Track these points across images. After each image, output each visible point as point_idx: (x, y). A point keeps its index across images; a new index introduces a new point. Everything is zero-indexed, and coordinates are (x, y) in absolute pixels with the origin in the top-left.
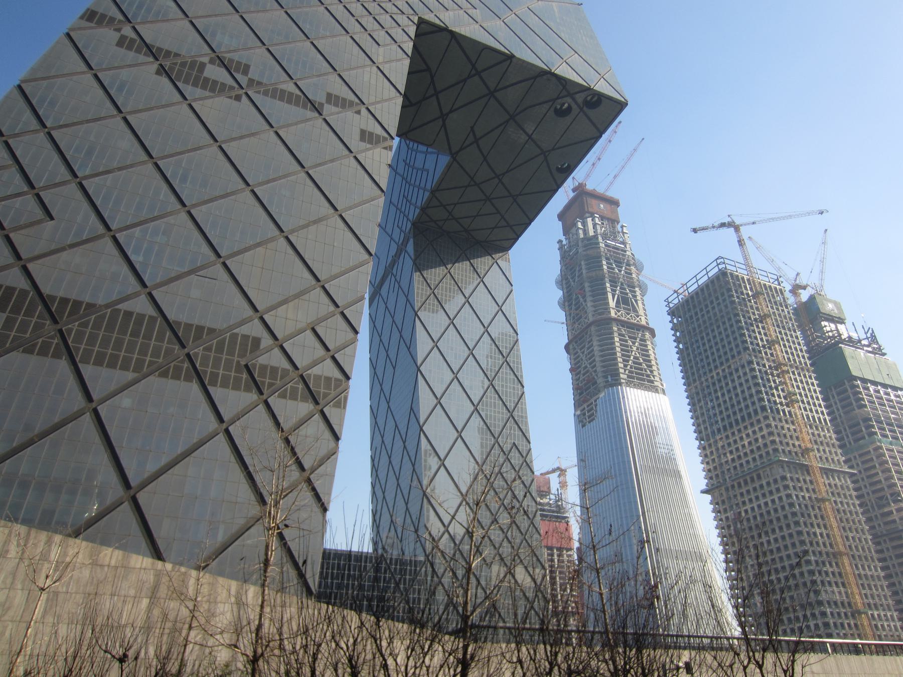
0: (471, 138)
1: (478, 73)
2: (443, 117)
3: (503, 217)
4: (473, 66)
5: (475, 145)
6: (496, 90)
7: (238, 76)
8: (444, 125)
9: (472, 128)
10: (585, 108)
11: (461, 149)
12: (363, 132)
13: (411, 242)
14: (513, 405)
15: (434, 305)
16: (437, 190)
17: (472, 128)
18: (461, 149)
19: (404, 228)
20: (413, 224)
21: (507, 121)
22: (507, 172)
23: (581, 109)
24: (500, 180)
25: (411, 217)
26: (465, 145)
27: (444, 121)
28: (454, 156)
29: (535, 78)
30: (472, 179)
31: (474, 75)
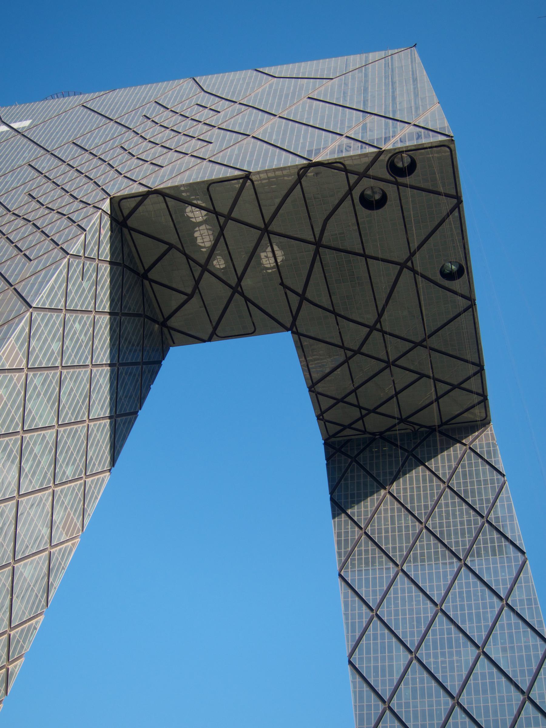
3: (435, 380)
5: (305, 302)
6: (267, 225)
8: (247, 299)
9: (282, 284)
10: (400, 180)
14: (528, 679)
17: (282, 284)
18: (295, 318)
21: (317, 252)
22: (380, 315)
27: (242, 294)
28: (292, 328)
29: (299, 181)
31: (226, 223)
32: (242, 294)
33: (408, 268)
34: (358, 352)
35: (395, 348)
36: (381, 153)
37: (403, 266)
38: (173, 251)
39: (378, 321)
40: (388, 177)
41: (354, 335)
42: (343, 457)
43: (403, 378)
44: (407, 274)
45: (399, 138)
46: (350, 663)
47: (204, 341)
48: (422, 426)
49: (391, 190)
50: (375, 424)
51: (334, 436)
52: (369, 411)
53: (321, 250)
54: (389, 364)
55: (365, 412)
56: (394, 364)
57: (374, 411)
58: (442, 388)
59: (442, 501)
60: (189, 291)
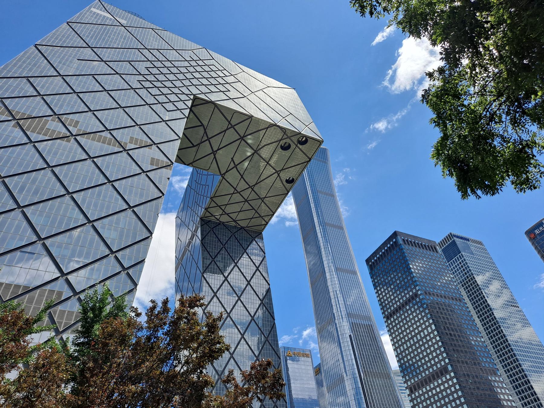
0: (232, 165)
1: (233, 127)
2: (214, 153)
3: (256, 212)
4: (229, 122)
6: (244, 136)
7: (70, 128)
8: (215, 157)
9: (232, 159)
10: (299, 145)
11: (227, 172)
12: (153, 159)
13: (200, 228)
15: (214, 268)
16: (214, 197)
18: (227, 172)
19: (195, 222)
20: (201, 219)
22: (256, 184)
23: (297, 145)
24: (253, 189)
25: (199, 214)
26: (229, 169)
27: (215, 155)
30: (235, 189)
32: (215, 155)
34: (239, 193)
37: (277, 172)
38: (202, 128)
41: (242, 185)
42: (208, 227)
43: (246, 206)
44: (276, 175)
47: (185, 164)
48: (239, 225)
49: (293, 146)
50: (224, 219)
54: (246, 201)
55: (224, 213)
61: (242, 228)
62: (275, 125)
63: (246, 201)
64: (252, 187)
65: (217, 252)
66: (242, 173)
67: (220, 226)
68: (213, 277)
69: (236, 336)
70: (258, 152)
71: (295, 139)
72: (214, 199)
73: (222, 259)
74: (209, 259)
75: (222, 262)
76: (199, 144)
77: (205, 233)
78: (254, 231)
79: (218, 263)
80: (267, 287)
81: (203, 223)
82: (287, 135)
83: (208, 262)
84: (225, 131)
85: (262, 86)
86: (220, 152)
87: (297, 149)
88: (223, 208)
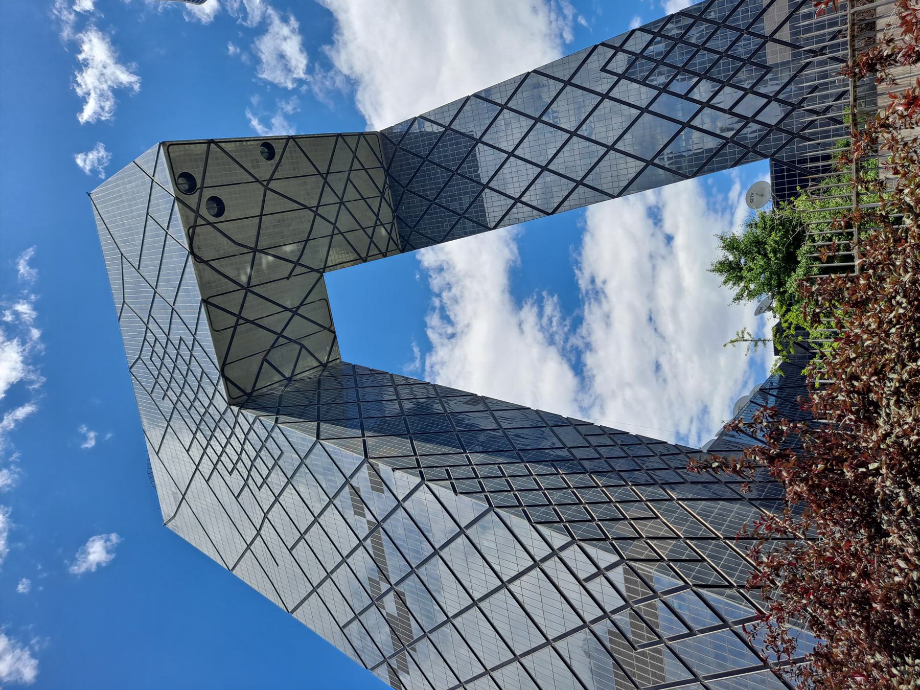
2: (295, 312)
3: (350, 170)
8: (302, 304)
10: (199, 186)
18: (313, 270)
21: (262, 251)
22: (306, 207)
23: (202, 188)
27: (298, 308)
28: (321, 272)
32: (298, 308)
33: (268, 184)
34: (334, 224)
35: (329, 197)
36: (177, 199)
37: (267, 188)
39: (310, 209)
40: (197, 194)
41: (323, 228)
42: (412, 237)
43: (351, 194)
44: (273, 185)
45: (164, 175)
46: (553, 212)
49: (208, 194)
50: (386, 214)
51: (397, 245)
52: (378, 219)
53: (259, 248)
54: (342, 203)
55: (378, 222)
56: (341, 199)
57: (377, 215)
58: (356, 165)
59: (437, 161)
60: (298, 347)
61: (387, 173)
62: (192, 252)
63: (342, 203)
64: (315, 211)
65: (446, 213)
66: (301, 245)
67: (401, 217)
68: (491, 210)
69: (576, 146)
70: (253, 246)
71: (192, 200)
72: (364, 255)
73: (455, 200)
74: (464, 223)
75: (460, 199)
76: (295, 342)
77: (424, 239)
78: (385, 149)
79: (465, 207)
80: (474, 101)
81: (408, 247)
82: (196, 221)
83: (469, 224)
84: (252, 322)
85: (130, 276)
86: (288, 304)
87: (208, 182)
88: (370, 231)
